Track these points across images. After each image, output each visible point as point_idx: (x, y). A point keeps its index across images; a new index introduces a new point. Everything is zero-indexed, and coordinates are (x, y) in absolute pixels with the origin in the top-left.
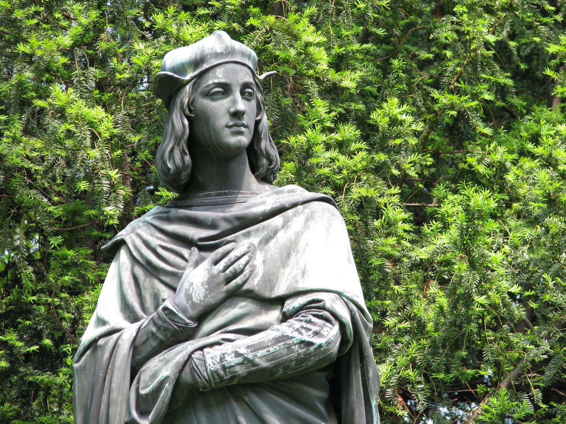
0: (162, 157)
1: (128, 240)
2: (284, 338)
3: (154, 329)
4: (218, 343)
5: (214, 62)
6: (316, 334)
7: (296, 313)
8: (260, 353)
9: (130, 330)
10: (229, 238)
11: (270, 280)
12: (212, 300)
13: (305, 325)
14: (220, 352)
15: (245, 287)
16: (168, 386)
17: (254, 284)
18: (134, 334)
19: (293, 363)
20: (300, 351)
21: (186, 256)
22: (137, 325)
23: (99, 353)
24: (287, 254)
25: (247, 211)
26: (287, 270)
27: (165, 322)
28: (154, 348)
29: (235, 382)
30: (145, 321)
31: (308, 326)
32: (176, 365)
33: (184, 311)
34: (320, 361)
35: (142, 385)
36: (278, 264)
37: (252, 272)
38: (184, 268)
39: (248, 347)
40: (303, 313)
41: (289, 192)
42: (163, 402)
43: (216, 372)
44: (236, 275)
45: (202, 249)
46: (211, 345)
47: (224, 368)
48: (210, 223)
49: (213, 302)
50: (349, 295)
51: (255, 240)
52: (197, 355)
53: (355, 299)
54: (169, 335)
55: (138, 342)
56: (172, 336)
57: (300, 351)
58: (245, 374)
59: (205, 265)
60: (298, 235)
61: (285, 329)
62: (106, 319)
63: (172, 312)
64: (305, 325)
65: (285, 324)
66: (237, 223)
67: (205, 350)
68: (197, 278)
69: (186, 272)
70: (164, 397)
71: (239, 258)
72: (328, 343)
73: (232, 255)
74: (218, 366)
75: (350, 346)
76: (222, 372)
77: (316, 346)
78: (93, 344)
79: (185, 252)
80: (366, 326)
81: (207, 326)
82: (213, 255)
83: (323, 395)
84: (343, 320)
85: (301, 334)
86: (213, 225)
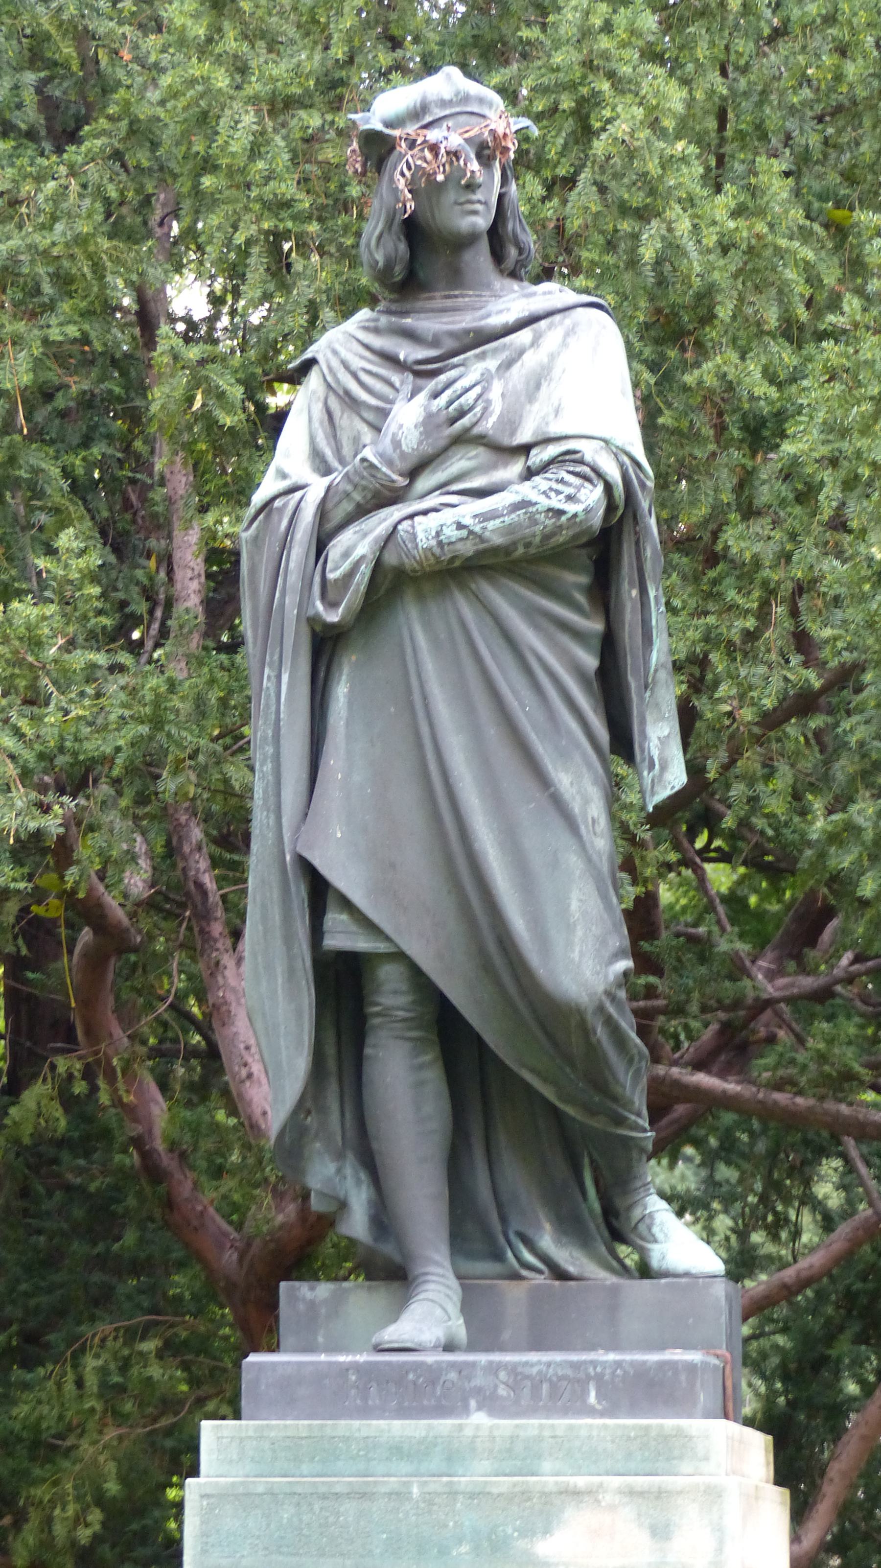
0: (368, 245)
1: (320, 358)
2: (524, 504)
3: (349, 488)
4: (435, 510)
5: (439, 113)
6: (570, 498)
7: (544, 467)
8: (492, 525)
9: (317, 488)
10: (455, 360)
11: (511, 422)
12: (428, 449)
13: (555, 486)
14: (437, 522)
15: (476, 431)
16: (365, 570)
17: (488, 425)
18: (322, 494)
19: (538, 539)
20: (548, 522)
21: (397, 384)
22: (327, 480)
23: (275, 517)
24: (536, 383)
25: (483, 323)
26: (536, 406)
27: (363, 478)
28: (349, 514)
29: (457, 563)
30: (336, 477)
31: (560, 487)
32: (376, 540)
33: (390, 463)
34: (575, 537)
35: (329, 565)
36: (523, 398)
37: (485, 409)
38: (392, 402)
39: (475, 516)
40: (553, 468)
41: (544, 293)
42: (357, 590)
43: (430, 549)
44: (462, 413)
45: (418, 374)
46: (425, 513)
47: (440, 544)
48: (430, 338)
49: (430, 451)
50: (619, 443)
51: (492, 364)
52: (406, 525)
53: (628, 448)
54: (369, 496)
55: (330, 505)
56: (373, 497)
57: (548, 522)
58: (471, 553)
59: (422, 398)
60: (552, 357)
61: (527, 491)
62: (287, 471)
63: (372, 466)
64: (555, 486)
65: (527, 484)
66: (467, 341)
67: (417, 519)
68: (408, 417)
69: (396, 408)
70: (358, 585)
71: (467, 390)
72: (587, 511)
73: (458, 386)
74: (433, 543)
75: (620, 512)
76: (437, 551)
77: (569, 515)
78: (268, 503)
79: (396, 379)
80: (643, 485)
81: (424, 483)
82: (432, 384)
83: (584, 579)
84: (609, 478)
85: (549, 497)
86: (435, 343)
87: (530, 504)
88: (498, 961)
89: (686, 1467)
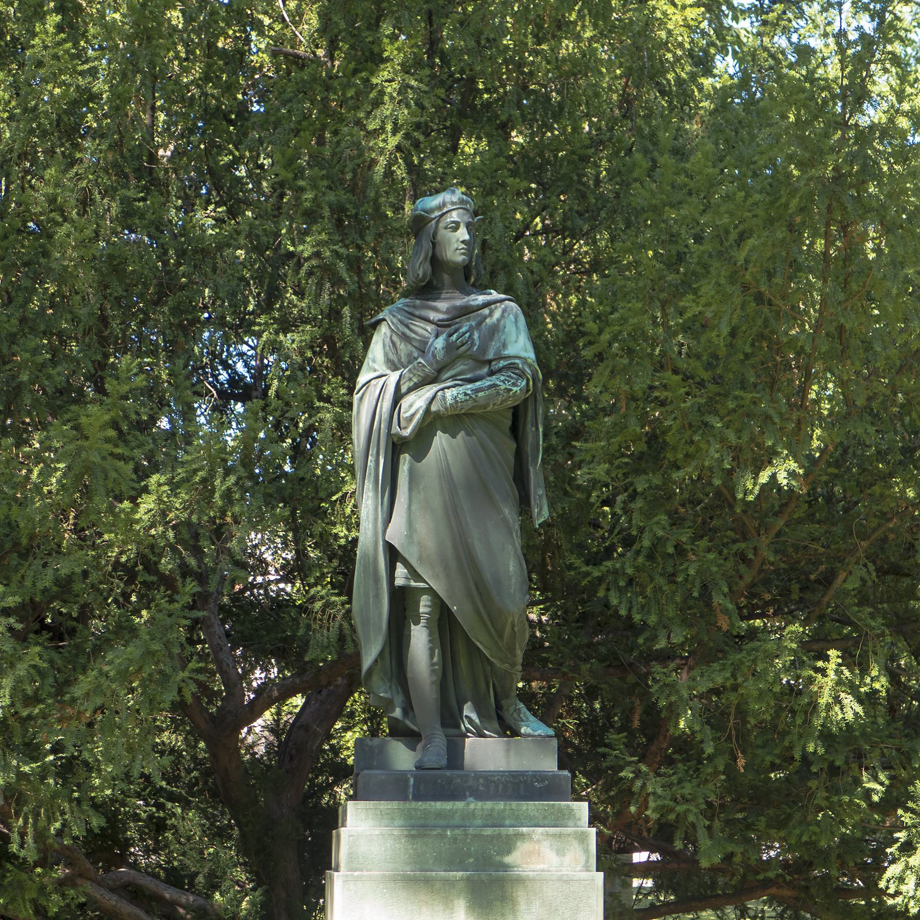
7: (500, 370)
8: (480, 394)
11: (484, 349)
60: (499, 320)
61: (493, 379)
71: (464, 333)
87: (497, 385)
88: (475, 593)
89: (570, 823)
